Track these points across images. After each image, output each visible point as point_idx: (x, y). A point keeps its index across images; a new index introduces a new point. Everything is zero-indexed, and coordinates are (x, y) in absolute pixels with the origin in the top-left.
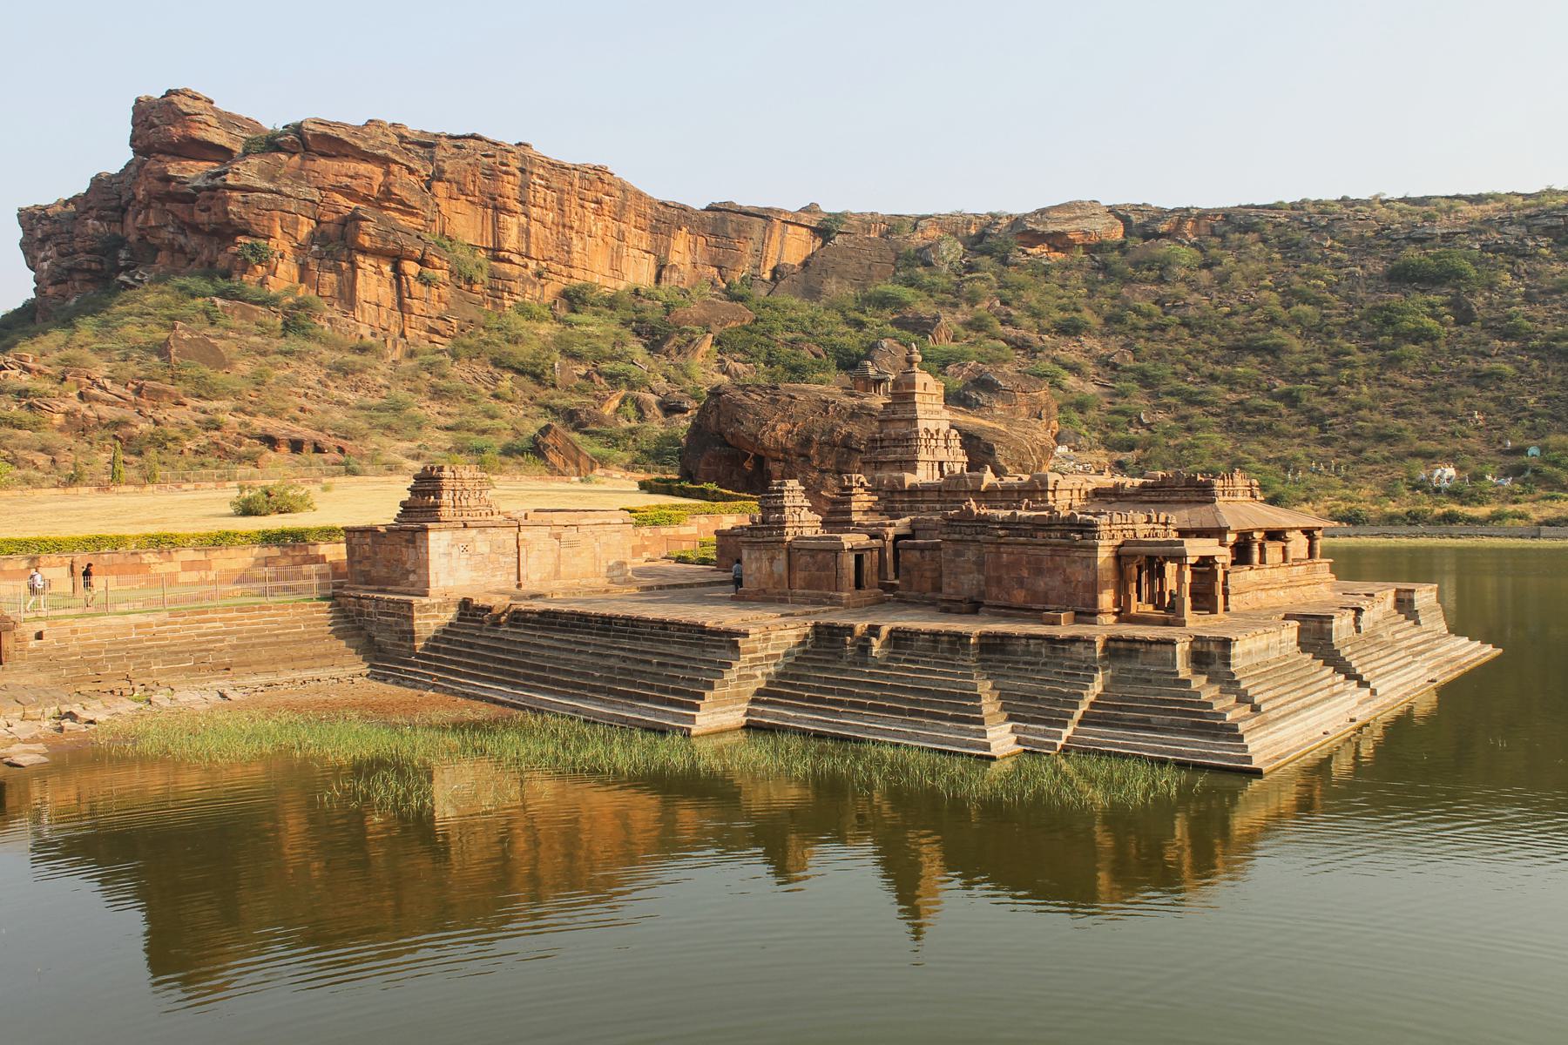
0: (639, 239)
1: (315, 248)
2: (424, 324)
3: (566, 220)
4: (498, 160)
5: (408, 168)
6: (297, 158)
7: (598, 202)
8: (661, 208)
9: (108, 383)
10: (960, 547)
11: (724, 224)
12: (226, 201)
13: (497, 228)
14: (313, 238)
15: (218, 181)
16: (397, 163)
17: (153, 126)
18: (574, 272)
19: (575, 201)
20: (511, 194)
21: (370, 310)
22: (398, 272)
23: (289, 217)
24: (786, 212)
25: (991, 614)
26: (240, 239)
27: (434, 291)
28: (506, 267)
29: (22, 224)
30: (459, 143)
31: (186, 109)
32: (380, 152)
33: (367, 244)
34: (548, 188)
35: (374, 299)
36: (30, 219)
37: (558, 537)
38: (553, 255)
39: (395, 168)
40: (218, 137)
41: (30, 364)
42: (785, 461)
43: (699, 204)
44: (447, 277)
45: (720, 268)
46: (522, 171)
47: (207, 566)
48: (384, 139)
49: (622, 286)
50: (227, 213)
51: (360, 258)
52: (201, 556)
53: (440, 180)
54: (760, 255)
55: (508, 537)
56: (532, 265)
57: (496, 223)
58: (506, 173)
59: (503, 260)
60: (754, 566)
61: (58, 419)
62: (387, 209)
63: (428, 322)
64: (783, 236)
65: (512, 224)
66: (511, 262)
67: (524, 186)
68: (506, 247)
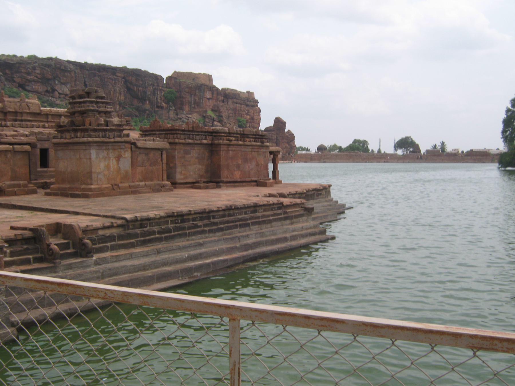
10: (188, 148)
25: (227, 187)
60: (102, 165)
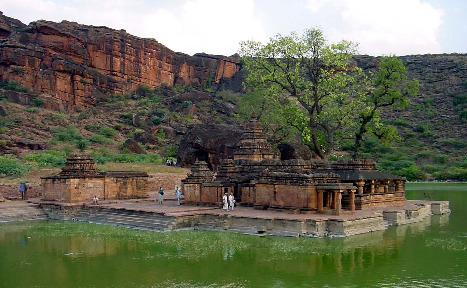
0: (167, 67)
1: (41, 70)
4: (113, 36)
5: (78, 39)
6: (35, 35)
7: (152, 53)
8: (176, 55)
11: (201, 62)
12: (6, 52)
15: (4, 44)
16: (73, 37)
18: (142, 80)
19: (143, 52)
20: (118, 49)
21: (62, 94)
22: (73, 80)
24: (226, 57)
26: (12, 66)
28: (115, 78)
32: (67, 33)
33: (61, 69)
34: (132, 47)
35: (64, 90)
39: (73, 39)
42: (215, 154)
43: (191, 53)
44: (92, 82)
45: (199, 78)
46: (122, 40)
48: (69, 28)
50: (7, 56)
51: (58, 74)
53: (90, 44)
54: (216, 74)
56: (126, 77)
57: (112, 60)
58: (116, 41)
59: (114, 75)
62: (69, 55)
63: (84, 99)
65: (118, 61)
66: (117, 75)
68: (116, 70)
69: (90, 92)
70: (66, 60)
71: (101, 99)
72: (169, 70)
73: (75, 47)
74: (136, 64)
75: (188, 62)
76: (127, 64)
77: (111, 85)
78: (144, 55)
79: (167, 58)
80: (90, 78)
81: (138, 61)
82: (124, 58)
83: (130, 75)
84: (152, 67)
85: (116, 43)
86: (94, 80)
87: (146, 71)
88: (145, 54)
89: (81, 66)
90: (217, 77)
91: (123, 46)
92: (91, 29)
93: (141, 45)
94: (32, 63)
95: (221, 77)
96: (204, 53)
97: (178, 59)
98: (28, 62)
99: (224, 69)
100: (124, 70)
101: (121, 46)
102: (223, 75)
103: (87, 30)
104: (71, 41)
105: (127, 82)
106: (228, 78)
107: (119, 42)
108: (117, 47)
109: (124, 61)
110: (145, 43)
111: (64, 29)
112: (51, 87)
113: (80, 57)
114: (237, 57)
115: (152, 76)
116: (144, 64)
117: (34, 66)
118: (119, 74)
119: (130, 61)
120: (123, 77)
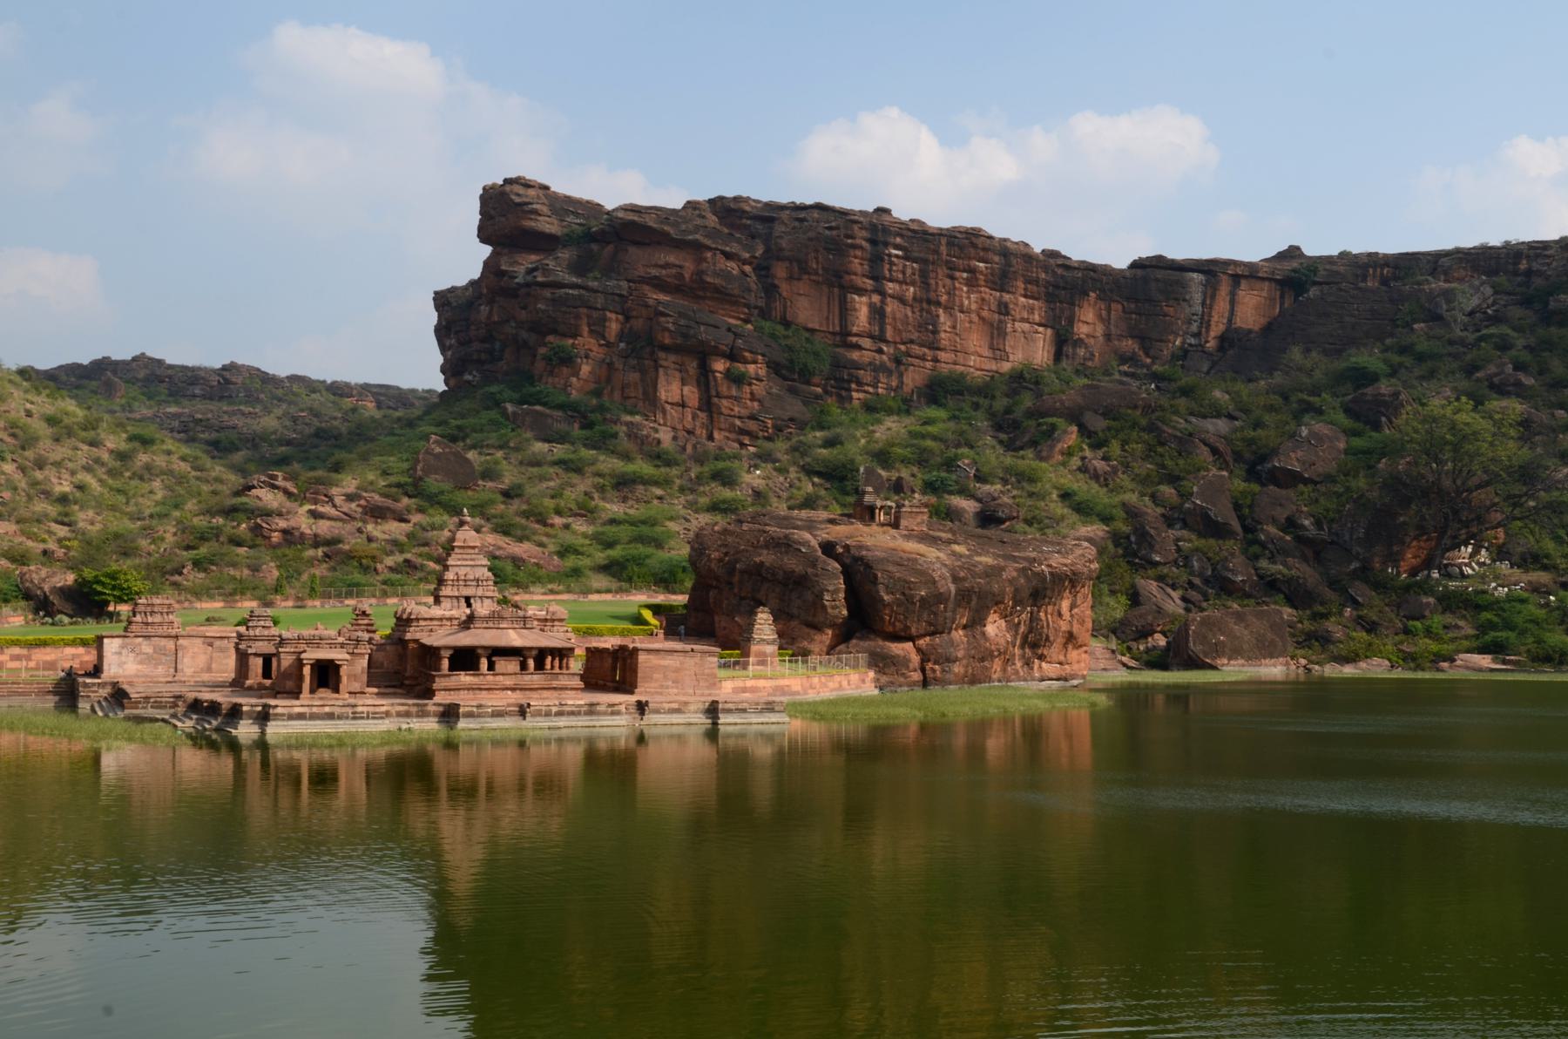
1: (622, 345)
2: (733, 425)
3: (932, 295)
4: (843, 231)
6: (610, 248)
7: (972, 271)
8: (1060, 271)
9: (338, 500)
13: (845, 311)
14: (621, 336)
16: (710, 249)
17: (492, 218)
18: (942, 355)
20: (859, 269)
21: (673, 412)
23: (595, 314)
26: (550, 338)
27: (747, 389)
28: (855, 355)
29: (437, 308)
30: (802, 215)
31: (517, 200)
33: (667, 341)
34: (906, 258)
36: (443, 300)
37: (211, 645)
38: (915, 336)
39: (709, 255)
40: (548, 225)
41: (280, 482)
43: (1119, 258)
44: (762, 372)
46: (873, 242)
47: (28, 658)
48: (699, 222)
49: (1006, 367)
51: (662, 355)
52: (24, 652)
53: (779, 259)
55: (170, 644)
58: (855, 247)
61: (276, 537)
63: (738, 422)
64: (1233, 294)
65: (861, 309)
66: (858, 347)
67: (876, 260)
68: (855, 330)
69: (756, 404)
70: (681, 315)
71: (791, 420)
72: (1037, 318)
73: (716, 274)
74: (922, 310)
75: (1102, 290)
76: (893, 313)
77: (842, 379)
78: (948, 282)
79: (1028, 281)
80: (755, 362)
81: (927, 302)
82: (882, 293)
83: (904, 343)
84: (975, 318)
85: (852, 252)
86: (775, 368)
87: (954, 327)
88: (952, 278)
89: (729, 330)
90: (1208, 331)
91: (876, 260)
92: (785, 215)
93: (936, 252)
94: (598, 332)
95: (1222, 328)
96: (1160, 258)
97: (1063, 283)
98: (589, 325)
99: (1233, 303)
100: (882, 330)
101: (870, 261)
102: (1230, 321)
103: (771, 220)
104: (705, 260)
105: (892, 366)
106: (1250, 331)
107: (861, 247)
108: (857, 264)
109: (883, 302)
110: (948, 244)
111: (683, 227)
112: (645, 393)
113: (736, 303)
114: (1293, 257)
115: (976, 342)
116: (946, 308)
117: (604, 338)
118: (866, 343)
119: (901, 300)
120: (880, 351)
